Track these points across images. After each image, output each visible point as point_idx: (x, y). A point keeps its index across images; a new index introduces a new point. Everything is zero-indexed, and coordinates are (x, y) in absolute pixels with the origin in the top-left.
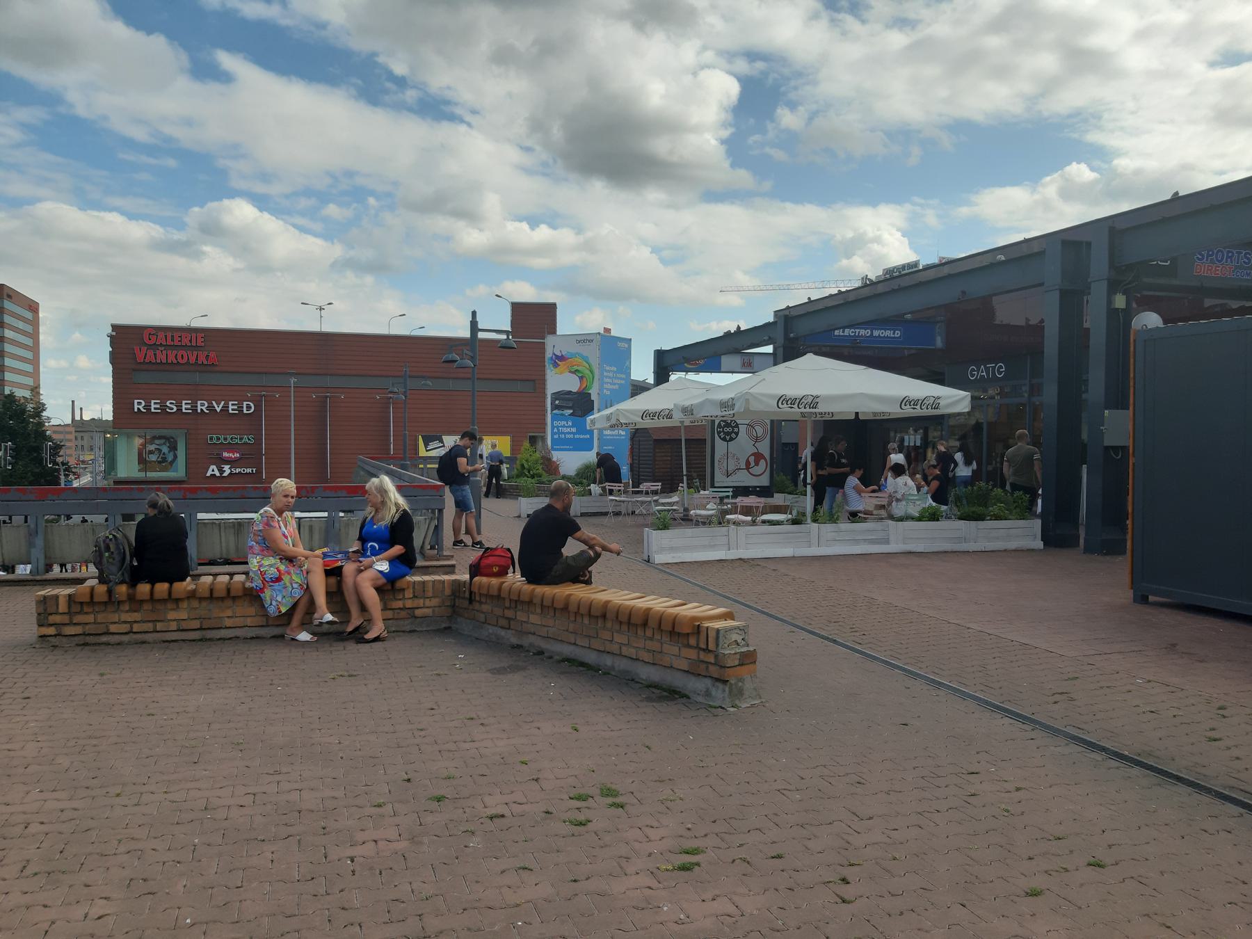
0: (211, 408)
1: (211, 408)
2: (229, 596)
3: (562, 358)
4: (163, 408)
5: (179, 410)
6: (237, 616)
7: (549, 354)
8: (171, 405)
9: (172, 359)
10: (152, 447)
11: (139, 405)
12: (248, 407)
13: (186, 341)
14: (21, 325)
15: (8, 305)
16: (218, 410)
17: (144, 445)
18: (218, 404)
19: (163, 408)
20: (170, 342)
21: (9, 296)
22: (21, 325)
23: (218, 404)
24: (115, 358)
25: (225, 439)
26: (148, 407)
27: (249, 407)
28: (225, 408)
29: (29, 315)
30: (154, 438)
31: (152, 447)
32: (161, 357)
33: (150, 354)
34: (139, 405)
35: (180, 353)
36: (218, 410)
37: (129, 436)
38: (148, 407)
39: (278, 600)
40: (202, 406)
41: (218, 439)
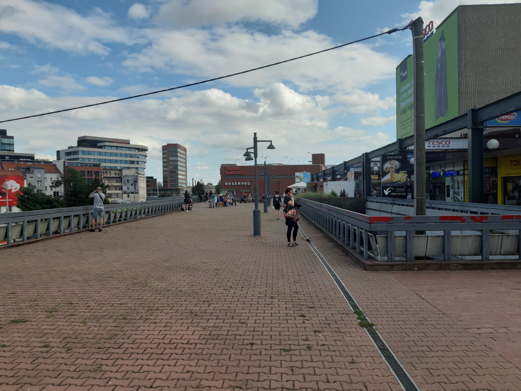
0: (241, 184)
1: (241, 184)
2: (247, 200)
3: (298, 176)
4: (231, 184)
5: (235, 185)
6: (248, 201)
7: (296, 176)
8: (233, 184)
9: (233, 173)
10: (229, 193)
11: (226, 184)
12: (249, 184)
13: (236, 169)
14: (182, 156)
15: (179, 150)
17: (227, 193)
19: (231, 184)
21: (179, 147)
22: (182, 156)
24: (221, 174)
26: (228, 184)
27: (249, 184)
28: (244, 184)
29: (184, 152)
30: (229, 191)
31: (229, 193)
32: (231, 173)
33: (228, 172)
34: (226, 184)
35: (235, 172)
37: (224, 191)
38: (228, 184)
39: (250, 200)
40: (239, 184)
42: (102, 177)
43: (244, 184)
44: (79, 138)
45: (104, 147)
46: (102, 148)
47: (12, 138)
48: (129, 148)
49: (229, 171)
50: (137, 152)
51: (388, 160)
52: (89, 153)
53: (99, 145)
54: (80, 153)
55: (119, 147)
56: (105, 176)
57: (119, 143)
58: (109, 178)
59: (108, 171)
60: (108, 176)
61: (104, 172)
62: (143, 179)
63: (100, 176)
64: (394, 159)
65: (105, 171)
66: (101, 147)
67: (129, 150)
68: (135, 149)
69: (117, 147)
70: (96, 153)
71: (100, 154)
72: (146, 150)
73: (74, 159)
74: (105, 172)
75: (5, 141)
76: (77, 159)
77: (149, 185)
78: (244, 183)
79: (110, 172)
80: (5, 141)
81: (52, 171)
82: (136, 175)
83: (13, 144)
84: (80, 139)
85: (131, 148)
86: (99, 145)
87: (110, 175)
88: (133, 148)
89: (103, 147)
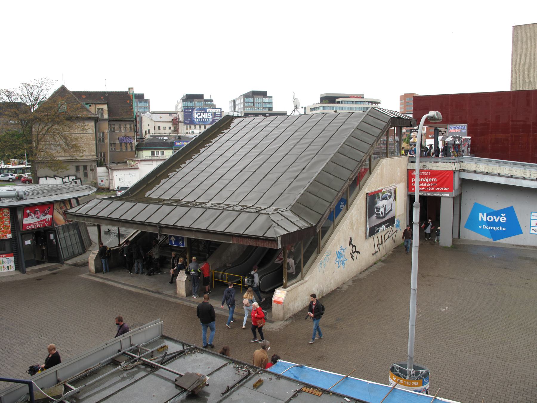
44: (321, 95)
46: (339, 104)
47: (271, 97)
48: (363, 102)
51: (413, 132)
53: (337, 100)
55: (354, 101)
64: (415, 131)
66: (338, 102)
68: (368, 102)
69: (352, 101)
70: (334, 108)
72: (380, 103)
75: (266, 100)
83: (272, 103)
84: (322, 96)
86: (337, 100)
88: (367, 102)
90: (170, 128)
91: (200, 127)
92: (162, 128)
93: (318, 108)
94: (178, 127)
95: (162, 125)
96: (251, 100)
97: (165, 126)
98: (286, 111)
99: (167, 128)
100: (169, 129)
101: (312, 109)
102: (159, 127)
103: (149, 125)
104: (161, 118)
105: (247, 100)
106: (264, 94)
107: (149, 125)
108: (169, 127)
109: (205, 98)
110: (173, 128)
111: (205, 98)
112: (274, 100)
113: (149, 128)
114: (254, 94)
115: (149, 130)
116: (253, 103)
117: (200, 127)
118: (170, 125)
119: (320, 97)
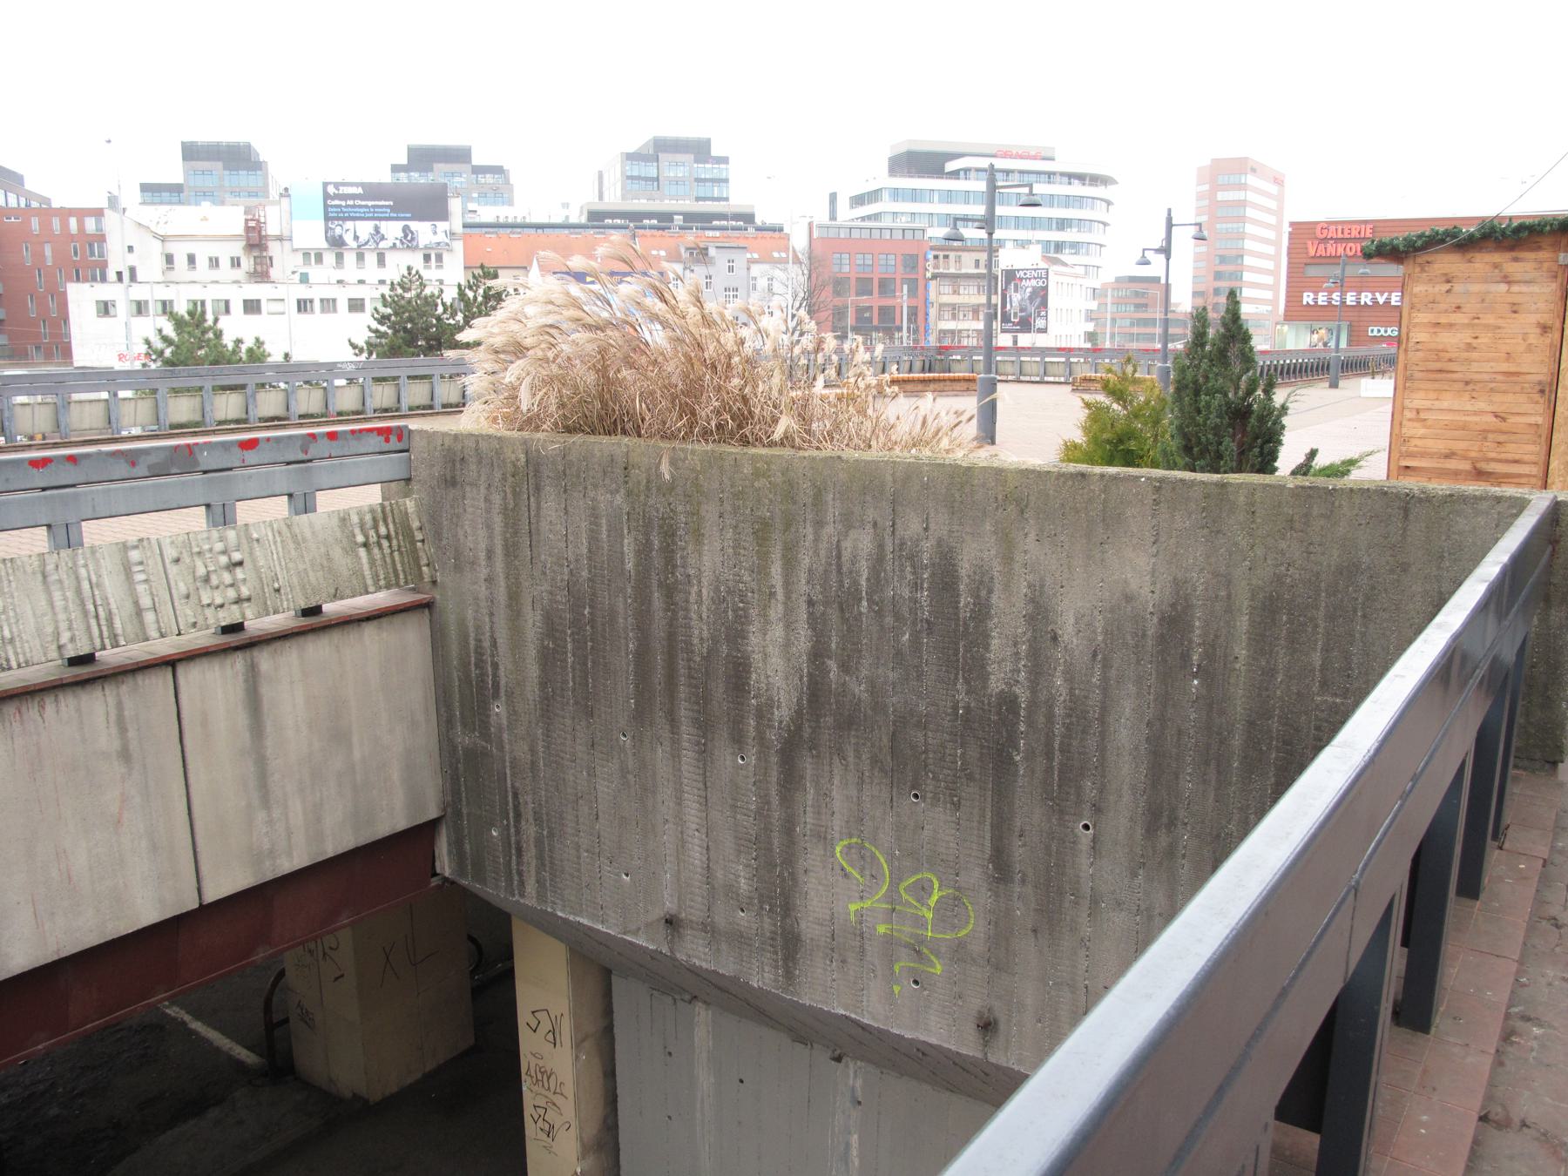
13: (1354, 234)
16: (1381, 303)
18: (1382, 295)
19: (1330, 299)
20: (1340, 236)
21: (1253, 170)
23: (1382, 295)
25: (1386, 331)
26: (1315, 300)
28: (1387, 302)
29: (1274, 189)
32: (1331, 249)
34: (1308, 298)
36: (1381, 303)
38: (1315, 300)
40: (1366, 298)
41: (1379, 331)
42: (929, 275)
43: (1387, 302)
45: (966, 174)
47: (725, 160)
49: (1325, 240)
50: (1077, 189)
52: (915, 195)
53: (951, 166)
54: (886, 195)
56: (941, 270)
57: (1035, 158)
58: (955, 277)
59: (952, 255)
60: (952, 270)
61: (936, 257)
62: (1071, 280)
63: (921, 270)
65: (941, 254)
66: (955, 174)
67: (1049, 182)
71: (949, 197)
73: (869, 218)
74: (941, 257)
75: (706, 171)
76: (876, 217)
77: (1146, 306)
78: (1389, 299)
79: (960, 257)
80: (706, 171)
81: (776, 255)
82: (1043, 265)
83: (726, 181)
85: (1054, 174)
86: (951, 166)
87: (960, 269)
89: (962, 173)
90: (236, 263)
91: (360, 257)
92: (202, 262)
93: (874, 196)
94: (271, 258)
95: (203, 253)
96: (651, 171)
97: (214, 255)
98: (753, 207)
99: (225, 263)
100: (233, 265)
101: (858, 200)
102: (191, 259)
103: (130, 249)
104: (205, 219)
105: (637, 169)
106: (699, 150)
107: (130, 249)
108: (232, 259)
109: (477, 160)
110: (247, 264)
111: (477, 160)
112: (733, 171)
113: (132, 260)
114: (663, 147)
115: (132, 270)
116: (657, 179)
117: (360, 257)
118: (237, 249)
119: (889, 154)
